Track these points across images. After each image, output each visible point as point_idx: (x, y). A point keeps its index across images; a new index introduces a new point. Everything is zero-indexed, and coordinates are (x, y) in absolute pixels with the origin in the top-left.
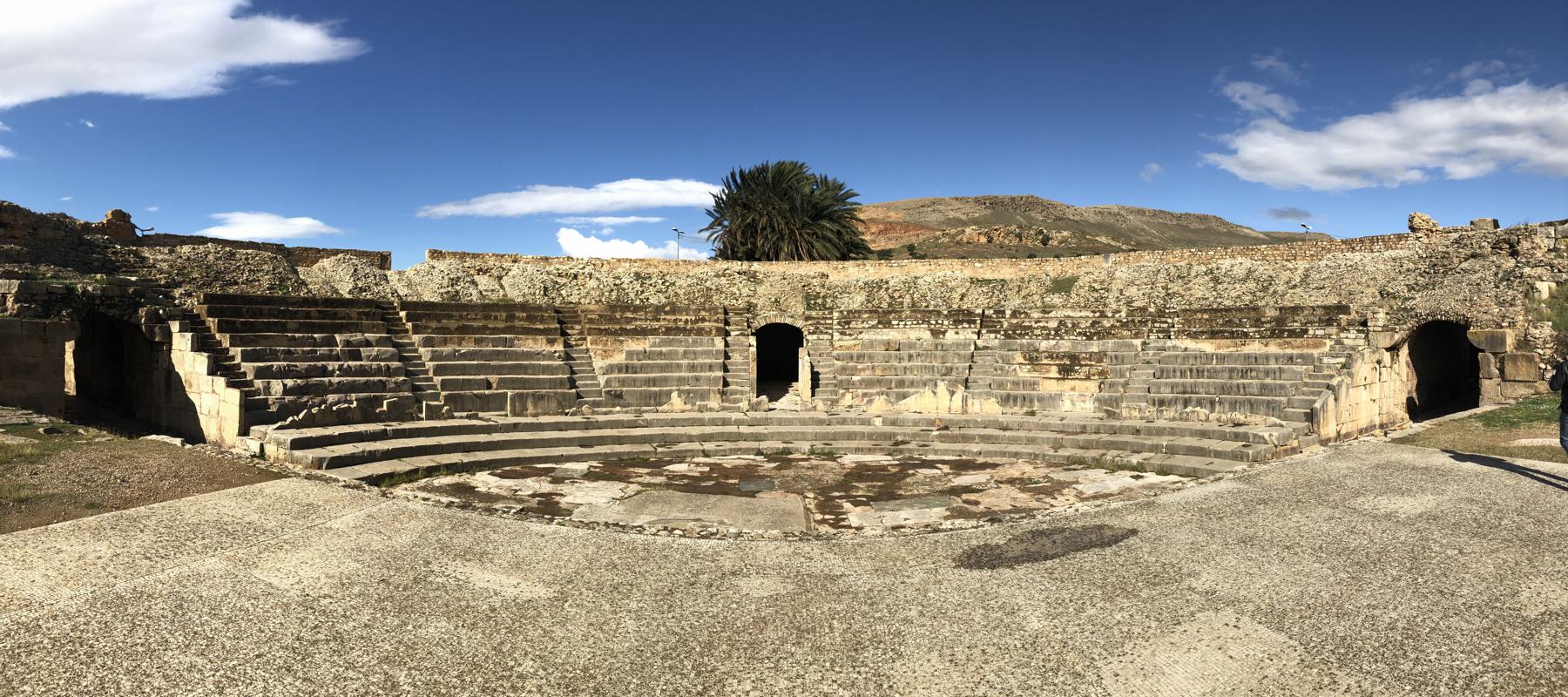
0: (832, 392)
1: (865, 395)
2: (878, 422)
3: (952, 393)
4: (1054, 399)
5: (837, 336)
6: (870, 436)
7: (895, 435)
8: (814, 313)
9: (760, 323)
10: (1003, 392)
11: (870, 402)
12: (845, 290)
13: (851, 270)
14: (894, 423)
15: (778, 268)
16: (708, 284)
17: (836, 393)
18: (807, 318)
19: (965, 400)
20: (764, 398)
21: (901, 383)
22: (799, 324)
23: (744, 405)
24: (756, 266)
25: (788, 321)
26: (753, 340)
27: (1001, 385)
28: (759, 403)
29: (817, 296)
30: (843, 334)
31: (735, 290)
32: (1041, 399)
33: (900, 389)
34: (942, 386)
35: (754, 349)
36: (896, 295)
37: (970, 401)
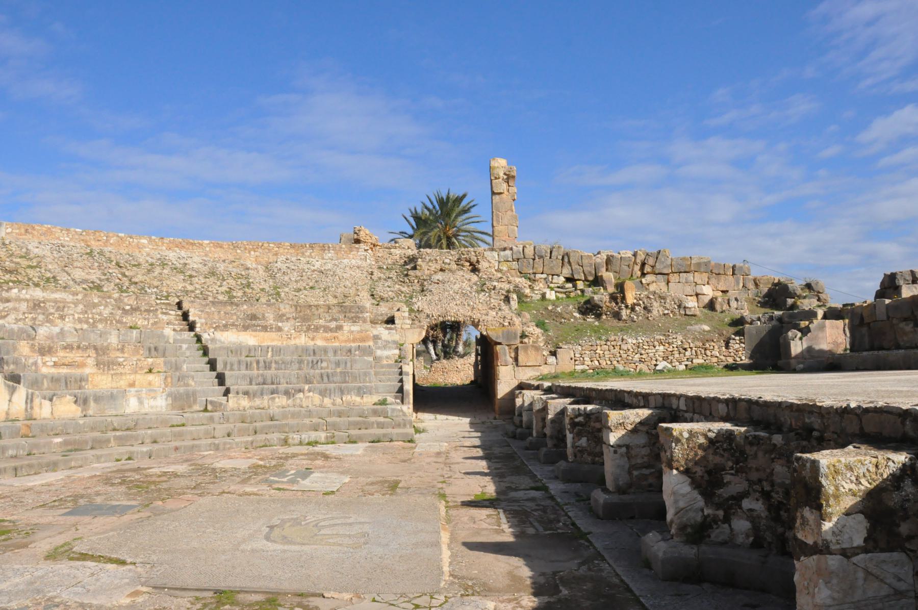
3: (12, 391)
19: (30, 400)
32: (97, 399)
37: (37, 401)
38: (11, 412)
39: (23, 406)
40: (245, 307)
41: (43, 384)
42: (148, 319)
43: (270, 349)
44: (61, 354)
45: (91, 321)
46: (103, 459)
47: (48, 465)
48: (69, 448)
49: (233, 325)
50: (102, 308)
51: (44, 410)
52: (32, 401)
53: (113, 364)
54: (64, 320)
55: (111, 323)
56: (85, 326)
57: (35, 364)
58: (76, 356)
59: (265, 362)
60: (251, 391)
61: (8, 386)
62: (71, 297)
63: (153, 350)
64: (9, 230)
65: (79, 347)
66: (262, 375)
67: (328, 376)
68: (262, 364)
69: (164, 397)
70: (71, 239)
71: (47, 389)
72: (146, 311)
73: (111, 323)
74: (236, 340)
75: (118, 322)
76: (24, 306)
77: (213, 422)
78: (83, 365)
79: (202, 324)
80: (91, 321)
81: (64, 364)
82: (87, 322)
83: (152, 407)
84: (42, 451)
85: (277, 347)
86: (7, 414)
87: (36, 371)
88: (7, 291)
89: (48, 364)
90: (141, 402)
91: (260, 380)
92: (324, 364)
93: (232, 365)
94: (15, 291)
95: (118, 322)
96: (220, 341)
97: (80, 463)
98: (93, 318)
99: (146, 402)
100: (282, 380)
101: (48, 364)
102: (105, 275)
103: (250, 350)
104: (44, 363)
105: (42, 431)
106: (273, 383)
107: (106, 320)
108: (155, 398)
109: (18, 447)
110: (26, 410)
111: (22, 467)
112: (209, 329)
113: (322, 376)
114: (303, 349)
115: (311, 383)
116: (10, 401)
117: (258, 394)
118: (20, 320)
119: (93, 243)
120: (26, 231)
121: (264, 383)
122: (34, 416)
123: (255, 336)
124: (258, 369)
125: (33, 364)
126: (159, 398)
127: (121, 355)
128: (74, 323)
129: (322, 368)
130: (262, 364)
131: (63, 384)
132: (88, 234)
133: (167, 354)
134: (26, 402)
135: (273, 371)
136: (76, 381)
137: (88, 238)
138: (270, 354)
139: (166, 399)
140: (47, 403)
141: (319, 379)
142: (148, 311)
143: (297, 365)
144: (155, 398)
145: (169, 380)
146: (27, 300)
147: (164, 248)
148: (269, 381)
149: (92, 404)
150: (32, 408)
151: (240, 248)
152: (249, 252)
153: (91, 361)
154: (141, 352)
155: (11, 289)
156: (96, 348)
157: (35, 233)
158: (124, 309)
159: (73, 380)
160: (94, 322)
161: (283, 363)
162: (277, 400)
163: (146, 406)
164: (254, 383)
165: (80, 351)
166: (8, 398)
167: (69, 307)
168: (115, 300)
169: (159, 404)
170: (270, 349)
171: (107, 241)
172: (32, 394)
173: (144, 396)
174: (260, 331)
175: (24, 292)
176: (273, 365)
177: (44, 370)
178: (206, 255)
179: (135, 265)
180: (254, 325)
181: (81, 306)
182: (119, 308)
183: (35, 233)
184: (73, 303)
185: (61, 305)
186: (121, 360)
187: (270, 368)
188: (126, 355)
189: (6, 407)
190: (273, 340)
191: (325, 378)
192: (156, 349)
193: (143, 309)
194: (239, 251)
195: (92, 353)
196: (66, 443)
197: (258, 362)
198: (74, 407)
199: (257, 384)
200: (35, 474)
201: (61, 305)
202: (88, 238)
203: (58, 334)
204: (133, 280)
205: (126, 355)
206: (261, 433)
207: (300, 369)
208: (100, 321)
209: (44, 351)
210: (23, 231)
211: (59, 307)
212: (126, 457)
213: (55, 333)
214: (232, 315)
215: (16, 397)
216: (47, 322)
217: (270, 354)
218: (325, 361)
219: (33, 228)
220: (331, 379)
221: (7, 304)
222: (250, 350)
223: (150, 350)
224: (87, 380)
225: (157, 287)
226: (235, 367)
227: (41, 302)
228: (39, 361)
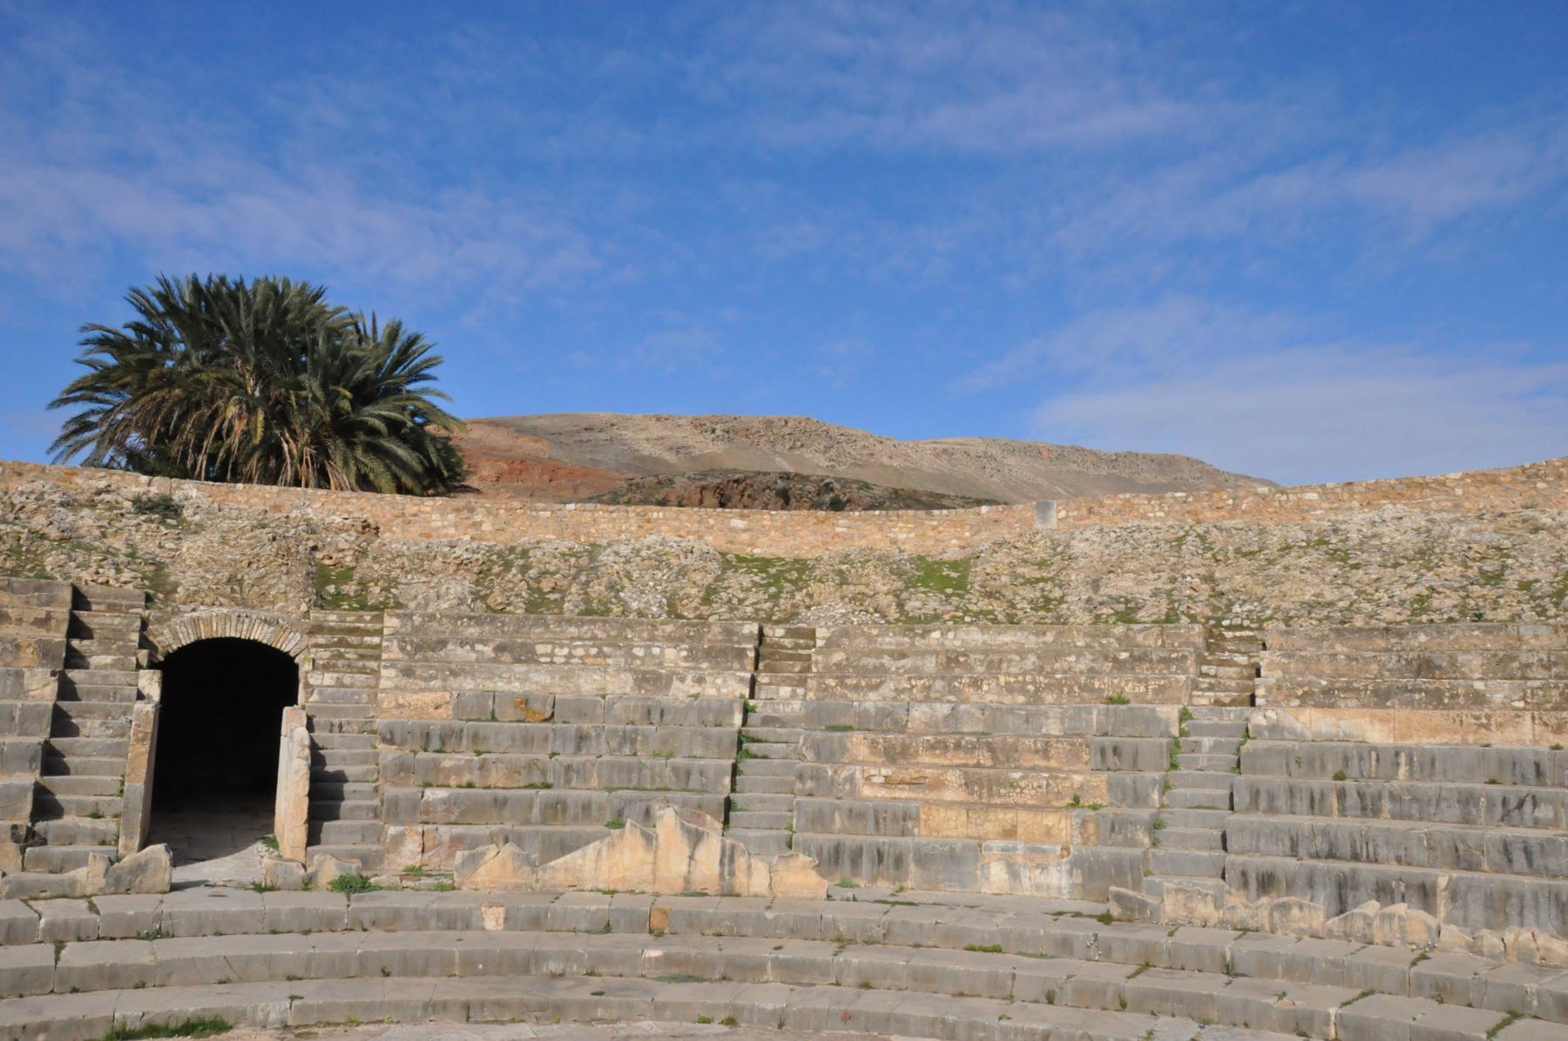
0: (365, 834)
1: (457, 841)
2: (492, 920)
3: (696, 838)
4: (956, 860)
5: (388, 677)
6: (469, 966)
7: (537, 958)
8: (332, 618)
9: (174, 635)
10: (826, 839)
11: (474, 861)
12: (421, 562)
13: (436, 520)
14: (535, 922)
15: (249, 499)
16: (39, 521)
17: (379, 834)
18: (317, 629)
19: (728, 858)
20: (158, 850)
21: (555, 810)
22: (288, 644)
23: (89, 874)
24: (189, 492)
25: (260, 634)
26: (151, 684)
27: (819, 820)
28: (140, 868)
29: (346, 575)
30: (408, 672)
31: (118, 544)
32: (923, 859)
33: (556, 826)
34: (668, 820)
35: (148, 709)
36: (546, 585)
37: (741, 862)
38: (694, 877)
39: (716, 869)
40: (1423, 638)
41: (833, 820)
42: (1146, 681)
43: (1403, 759)
44: (925, 758)
45: (1031, 688)
46: (668, 1013)
47: (542, 1007)
48: (675, 971)
49: (1348, 689)
50: (1073, 658)
51: (756, 878)
52: (732, 860)
53: (1000, 784)
54: (980, 687)
55: (1071, 691)
56: (1021, 699)
57: (851, 779)
59: (1361, 795)
60: (1280, 874)
61: (687, 831)
62: (1033, 638)
63: (1110, 753)
64: (1063, 514)
65: (958, 746)
66: (1325, 832)
67: (1527, 852)
68: (1352, 799)
69: (1065, 868)
70: (1167, 514)
71: (840, 832)
72: (1162, 660)
73: (1071, 691)
74: (1334, 730)
75: (1083, 688)
76: (930, 664)
77: (1071, 953)
78: (939, 785)
79: (1269, 690)
80: (1031, 688)
81: (902, 782)
82: (1023, 691)
83: (1038, 887)
84: (620, 970)
85: (1423, 752)
86: (687, 880)
87: (854, 791)
88: (923, 636)
89: (875, 780)
90: (1014, 874)
91: (1321, 845)
92: (1544, 812)
93: (1272, 798)
94: (936, 635)
95: (1083, 688)
96: (1292, 731)
97: (614, 1013)
98: (1034, 682)
99: (1025, 874)
100: (1383, 852)
101: (875, 780)
103: (1346, 760)
104: (868, 779)
105: (691, 925)
106: (1356, 857)
107: (1059, 686)
108: (1044, 868)
109: (567, 957)
110: (721, 875)
111: (483, 1005)
112: (1287, 698)
113: (1506, 849)
114: (1501, 763)
115: (1472, 867)
116: (691, 857)
117: (1301, 882)
118: (904, 690)
119: (1208, 514)
120: (1090, 511)
121: (1331, 855)
122: (737, 891)
123: (1383, 721)
124: (1343, 811)
125: (846, 780)
126: (1053, 869)
127: (1043, 763)
128: (998, 694)
129: (1536, 823)
130: (1352, 799)
131: (871, 823)
132: (1198, 499)
133: (1140, 766)
134: (722, 863)
135: (1383, 823)
136: (895, 819)
137: (1198, 506)
138: (1403, 770)
139: (1070, 873)
141: (1499, 858)
142: (1166, 661)
143: (1456, 811)
144: (1044, 868)
145: (1091, 828)
146: (936, 653)
147: (1355, 504)
148: (1346, 850)
149: (913, 868)
150: (732, 873)
151: (1543, 478)
153: (953, 777)
154: (1086, 757)
155: (926, 632)
156: (991, 749)
157: (1105, 511)
158: (1115, 660)
159: (889, 816)
160: (1037, 690)
161: (1415, 799)
162: (1295, 912)
163: (1026, 882)
164: (1302, 851)
165: (961, 754)
166: (687, 852)
167: (1010, 661)
168: (1119, 639)
169: (1057, 881)
170: (1403, 759)
171: (1235, 507)
172: (733, 847)
173: (1020, 860)
174: (1420, 705)
175: (951, 635)
176: (1386, 805)
177: (867, 791)
178: (1457, 506)
180: (1405, 689)
181: (1032, 658)
182: (1106, 658)
183: (1105, 511)
184: (1016, 652)
185: (996, 657)
187: (1376, 813)
188: (1053, 763)
189: (684, 868)
190: (1435, 731)
191: (1519, 859)
192: (1116, 751)
193: (1154, 657)
194: (1541, 485)
196: (667, 960)
197: (1342, 795)
198: (813, 878)
199: (1311, 856)
200: (513, 1021)
201: (996, 657)
202: (1198, 506)
203: (946, 717)
206: (1139, 1008)
207: (1466, 820)
208: (1049, 687)
210: (1084, 511)
211: (991, 662)
212: (724, 1016)
213: (940, 716)
214: (1367, 661)
215: (701, 853)
216: (950, 692)
217: (1403, 770)
218: (1549, 801)
219: (1102, 505)
220: (1538, 861)
221: (902, 662)
222: (1346, 760)
223: (1103, 752)
224: (917, 818)
225: (1260, 600)
226: (1282, 803)
227: (959, 654)
228: (858, 775)
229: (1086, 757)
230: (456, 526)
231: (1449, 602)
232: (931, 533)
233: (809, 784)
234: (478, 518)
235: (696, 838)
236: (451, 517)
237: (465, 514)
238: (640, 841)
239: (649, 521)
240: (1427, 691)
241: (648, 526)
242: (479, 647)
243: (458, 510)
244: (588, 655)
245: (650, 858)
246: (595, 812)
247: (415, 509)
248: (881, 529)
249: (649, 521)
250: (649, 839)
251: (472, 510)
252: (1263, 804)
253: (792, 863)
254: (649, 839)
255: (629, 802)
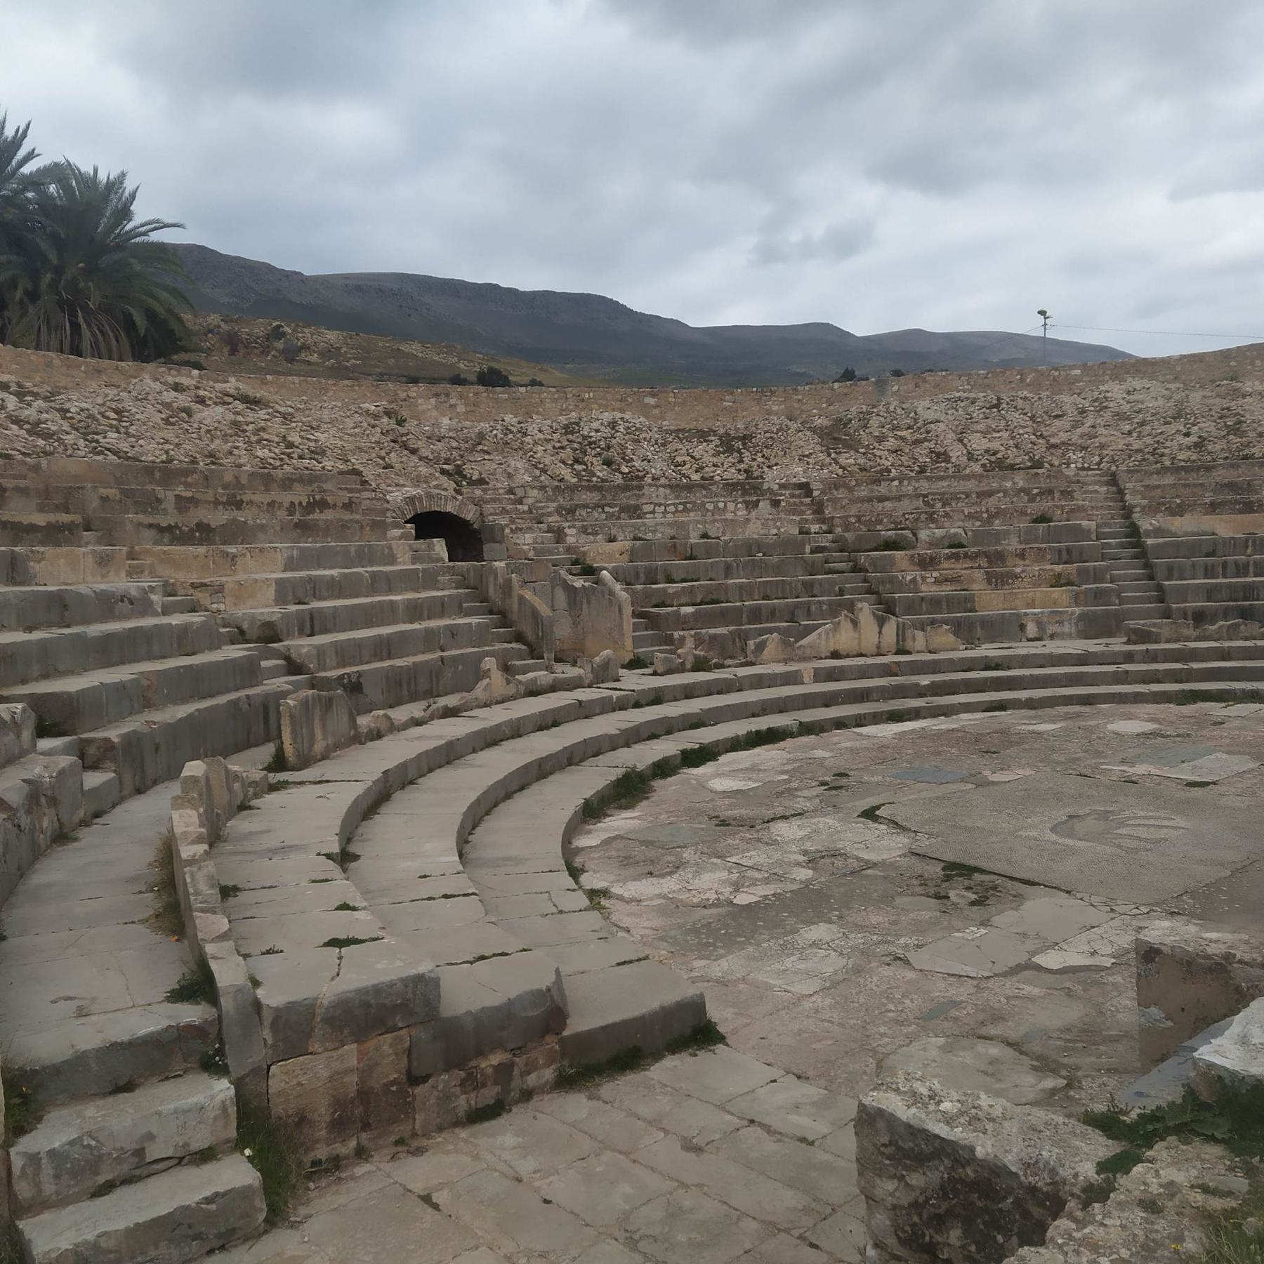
3: (881, 622)
44: (945, 565)
58: (960, 568)
64: (895, 388)
86: (878, 647)
102: (1013, 438)
116: (880, 632)
120: (917, 385)
127: (1022, 562)
139: (1076, 624)
140: (919, 634)
150: (904, 640)
152: (1252, 364)
153: (979, 574)
162: (1243, 627)
174: (1241, 512)
176: (1251, 569)
179: (1057, 417)
186: (1018, 570)
189: (876, 641)
195: (983, 562)
204: (1052, 441)
205: (1027, 562)
209: (925, 563)
210: (911, 386)
229: (1049, 557)
230: (436, 408)
231: (1218, 447)
232: (796, 405)
233: (888, 586)
234: (453, 401)
235: (881, 622)
236: (433, 401)
237: (443, 398)
238: (850, 625)
239: (583, 400)
240: (1244, 503)
241: (581, 405)
242: (607, 509)
243: (437, 395)
244: (677, 511)
245: (856, 636)
246: (778, 614)
247: (403, 395)
248: (759, 401)
249: (583, 400)
250: (855, 623)
251: (447, 395)
252: (1176, 575)
253: (940, 630)
254: (855, 623)
255: (797, 605)
